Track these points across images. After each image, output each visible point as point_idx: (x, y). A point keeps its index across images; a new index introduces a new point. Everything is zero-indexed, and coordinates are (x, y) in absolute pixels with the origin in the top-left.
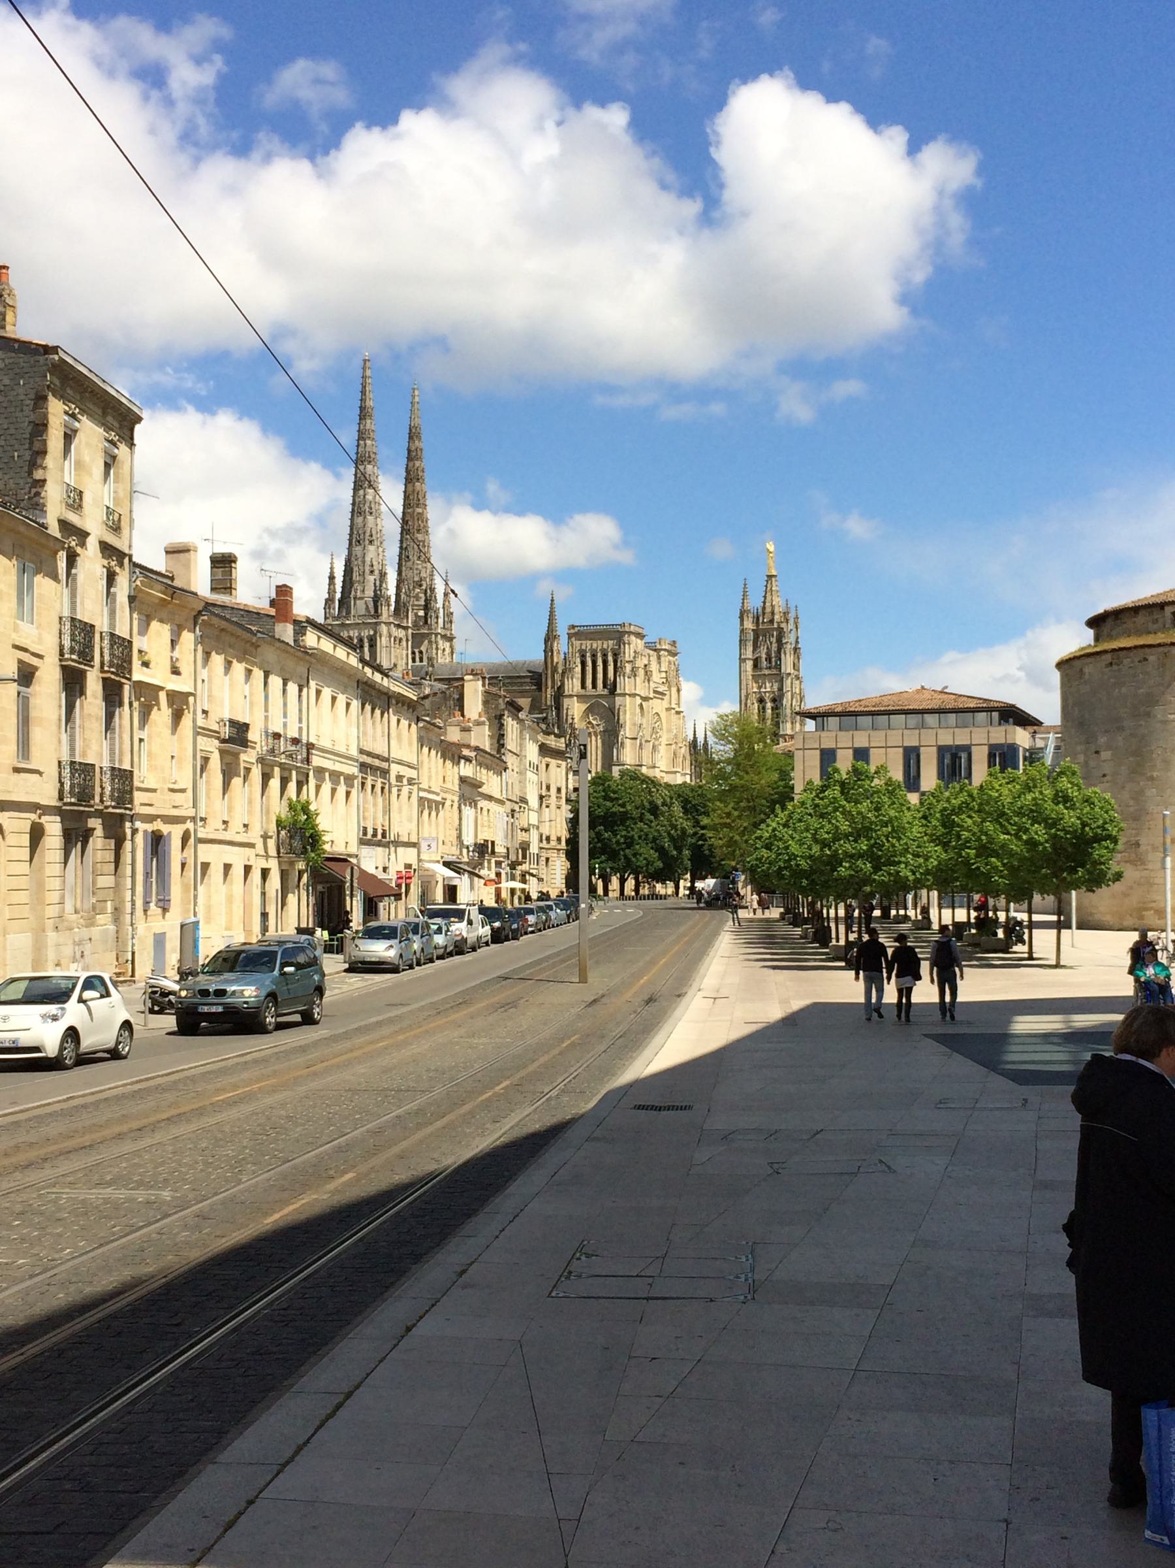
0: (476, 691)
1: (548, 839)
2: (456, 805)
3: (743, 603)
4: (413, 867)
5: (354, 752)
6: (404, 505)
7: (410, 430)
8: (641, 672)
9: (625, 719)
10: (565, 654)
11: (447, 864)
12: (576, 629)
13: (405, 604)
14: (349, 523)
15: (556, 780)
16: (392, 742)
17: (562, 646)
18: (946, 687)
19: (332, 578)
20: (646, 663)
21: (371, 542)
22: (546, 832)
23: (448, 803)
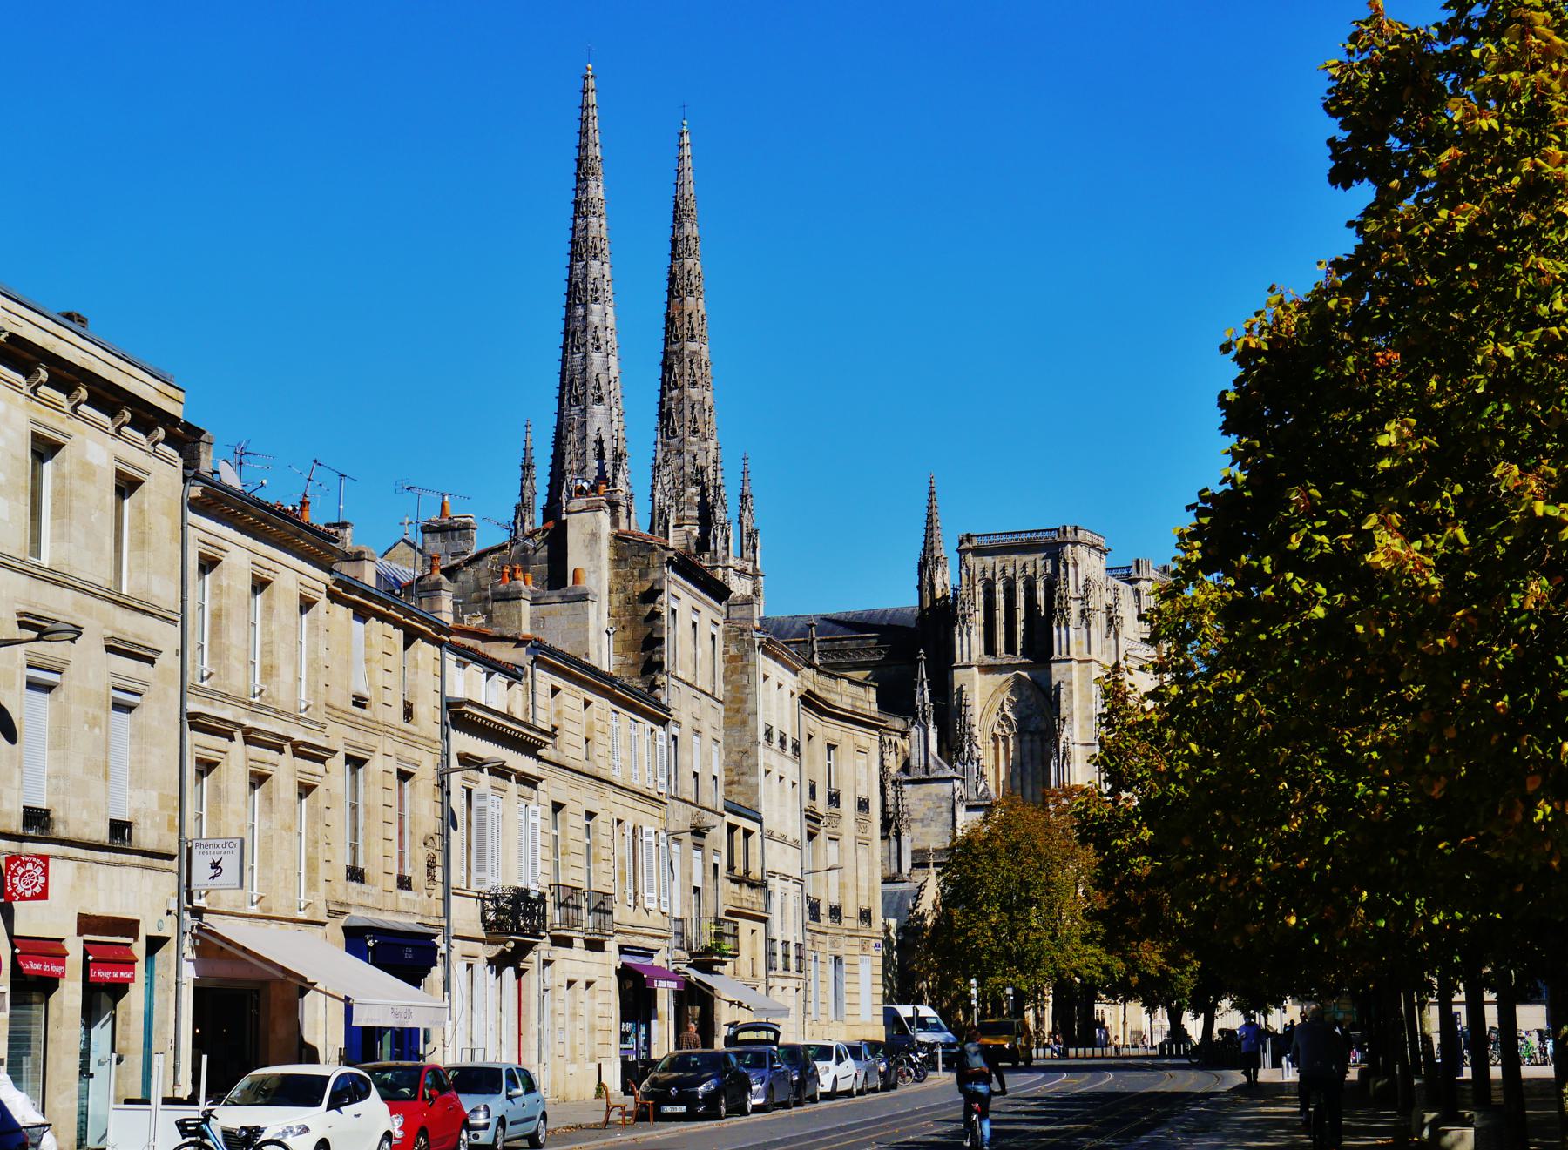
0: (594, 536)
1: (836, 912)
6: (666, 340)
7: (677, 206)
8: (1099, 619)
9: (1070, 707)
10: (954, 589)
11: (357, 940)
12: (975, 541)
13: (662, 512)
17: (945, 580)
19: (527, 467)
20: (1111, 602)
21: (600, 400)
22: (828, 896)
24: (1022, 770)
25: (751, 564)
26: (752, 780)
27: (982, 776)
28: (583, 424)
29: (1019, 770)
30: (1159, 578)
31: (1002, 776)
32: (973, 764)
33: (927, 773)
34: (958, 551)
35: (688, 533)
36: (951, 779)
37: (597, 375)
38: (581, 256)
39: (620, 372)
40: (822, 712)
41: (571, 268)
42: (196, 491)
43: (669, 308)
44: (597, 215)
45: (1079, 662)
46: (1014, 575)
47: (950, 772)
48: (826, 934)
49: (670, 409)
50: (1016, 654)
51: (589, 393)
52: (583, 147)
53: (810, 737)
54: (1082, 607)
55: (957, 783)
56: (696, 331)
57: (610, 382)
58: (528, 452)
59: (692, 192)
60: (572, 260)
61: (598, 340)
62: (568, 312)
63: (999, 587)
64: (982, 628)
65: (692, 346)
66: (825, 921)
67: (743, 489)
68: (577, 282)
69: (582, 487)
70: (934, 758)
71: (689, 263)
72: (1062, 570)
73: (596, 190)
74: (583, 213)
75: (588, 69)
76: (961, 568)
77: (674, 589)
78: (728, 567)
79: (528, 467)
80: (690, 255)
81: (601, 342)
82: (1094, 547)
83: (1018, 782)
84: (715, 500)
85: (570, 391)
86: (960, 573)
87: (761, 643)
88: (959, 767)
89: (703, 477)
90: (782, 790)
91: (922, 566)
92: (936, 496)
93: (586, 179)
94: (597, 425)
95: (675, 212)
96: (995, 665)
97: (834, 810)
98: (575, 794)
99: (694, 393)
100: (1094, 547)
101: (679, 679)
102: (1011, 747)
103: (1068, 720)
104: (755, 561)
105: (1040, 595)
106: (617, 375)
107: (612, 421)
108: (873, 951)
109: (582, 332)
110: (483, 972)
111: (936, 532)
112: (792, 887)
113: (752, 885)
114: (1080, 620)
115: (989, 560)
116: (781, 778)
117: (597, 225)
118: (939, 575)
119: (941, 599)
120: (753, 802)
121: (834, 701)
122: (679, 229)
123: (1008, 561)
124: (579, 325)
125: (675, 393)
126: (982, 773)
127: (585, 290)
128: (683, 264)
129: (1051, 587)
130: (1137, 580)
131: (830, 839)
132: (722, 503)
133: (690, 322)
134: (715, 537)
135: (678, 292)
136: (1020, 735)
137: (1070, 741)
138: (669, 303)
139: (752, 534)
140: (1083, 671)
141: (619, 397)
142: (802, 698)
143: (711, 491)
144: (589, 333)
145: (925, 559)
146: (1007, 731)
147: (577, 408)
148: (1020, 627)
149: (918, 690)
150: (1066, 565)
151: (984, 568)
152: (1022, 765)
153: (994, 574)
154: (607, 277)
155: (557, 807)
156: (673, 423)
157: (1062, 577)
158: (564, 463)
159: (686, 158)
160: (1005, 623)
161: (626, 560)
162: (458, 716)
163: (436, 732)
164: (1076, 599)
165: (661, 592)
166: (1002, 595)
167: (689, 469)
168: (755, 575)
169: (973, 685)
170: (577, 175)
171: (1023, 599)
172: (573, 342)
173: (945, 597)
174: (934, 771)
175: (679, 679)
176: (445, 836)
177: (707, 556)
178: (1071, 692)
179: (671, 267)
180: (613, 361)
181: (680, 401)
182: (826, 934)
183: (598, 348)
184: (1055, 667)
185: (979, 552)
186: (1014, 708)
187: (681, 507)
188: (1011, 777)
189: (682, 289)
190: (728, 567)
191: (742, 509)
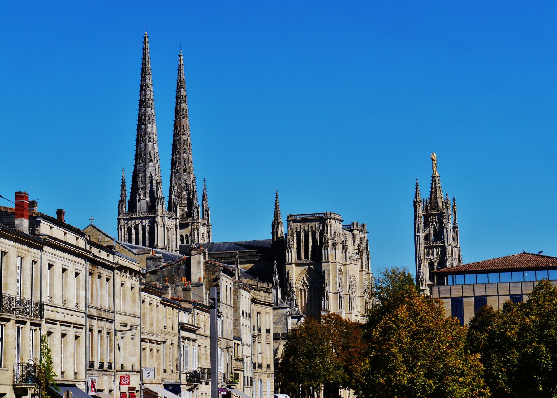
0: (199, 262)
1: (260, 366)
2: (176, 343)
3: (416, 197)
4: (136, 389)
5: (82, 307)
6: (174, 135)
7: (178, 83)
8: (339, 246)
9: (329, 279)
10: (286, 235)
11: (166, 387)
12: (294, 217)
13: (175, 203)
14: (135, 148)
15: (266, 324)
16: (117, 301)
17: (283, 230)
18: (541, 252)
19: (123, 186)
20: (344, 239)
21: (151, 161)
22: (258, 361)
23: (168, 342)
24: (311, 303)
25: (207, 221)
26: (239, 328)
27: (297, 306)
28: (145, 170)
29: (310, 302)
30: (361, 229)
31: (303, 305)
32: (293, 301)
33: (277, 305)
34: (287, 220)
36: (286, 308)
37: (150, 152)
38: (144, 106)
39: (158, 150)
40: (256, 303)
41: (140, 110)
42: (143, 287)
43: (175, 123)
44: (150, 90)
45: (332, 262)
46: (308, 230)
47: (286, 305)
48: (257, 373)
49: (176, 162)
51: (147, 159)
52: (144, 64)
53: (253, 311)
54: (333, 242)
55: (288, 309)
56: (186, 132)
57: (155, 154)
58: (123, 180)
59: (184, 78)
60: (140, 107)
61: (150, 138)
62: (138, 127)
63: (302, 234)
64: (296, 250)
65: (185, 138)
66: (257, 369)
67: (204, 192)
68: (142, 116)
69: (195, 247)
70: (280, 300)
71: (183, 106)
72: (326, 229)
74: (144, 89)
75: (145, 34)
76: (288, 227)
77: (222, 277)
78: (198, 223)
79: (123, 186)
80: (183, 103)
81: (151, 139)
82: (338, 219)
83: (309, 307)
84: (193, 197)
85: (140, 158)
86: (288, 229)
87: (241, 286)
88: (289, 302)
89: (188, 188)
90: (246, 329)
91: (273, 225)
92: (279, 199)
93: (145, 77)
94: (150, 171)
95: (177, 86)
96: (301, 263)
97: (259, 333)
98: (202, 342)
99: (185, 156)
100: (338, 219)
101: (223, 303)
102: (307, 294)
103: (328, 284)
104: (208, 220)
105: (318, 237)
106: (157, 151)
107: (156, 169)
108: (271, 378)
109: (144, 135)
110: (186, 392)
111: (278, 213)
112: (249, 359)
113: (240, 361)
114: (332, 247)
115: (299, 224)
116: (246, 326)
117: (149, 94)
118: (280, 228)
119: (280, 237)
120: (239, 335)
121: (259, 299)
122: (179, 92)
123: (306, 225)
124: (143, 133)
125: (178, 156)
126: (297, 305)
127: (145, 119)
128: (181, 106)
129: (322, 234)
130: (353, 230)
131: (258, 343)
132: (196, 198)
133: (183, 129)
135: (179, 117)
137: (329, 292)
138: (175, 121)
139: (207, 210)
140: (334, 266)
141: (158, 160)
142: (251, 300)
143: (192, 194)
144: (147, 135)
146: (305, 288)
147: (142, 164)
148: (310, 249)
149: (274, 275)
151: (297, 227)
152: (311, 300)
153: (300, 230)
154: (154, 114)
155: (199, 346)
156: (177, 167)
157: (326, 231)
158: (137, 185)
159: (181, 65)
160: (305, 248)
161: (208, 269)
162: (182, 327)
163: (176, 331)
164: (331, 239)
165: (219, 279)
166: (303, 237)
167: (183, 185)
168: (208, 225)
169: (293, 270)
170: (142, 75)
171: (311, 239)
172: (141, 139)
173: (282, 237)
174: (280, 305)
175: (223, 303)
176: (179, 358)
177: (191, 218)
178: (329, 274)
179: (176, 107)
180: (156, 146)
181: (180, 159)
182: (257, 373)
183: (150, 141)
184: (323, 264)
185: (295, 221)
186: (307, 280)
187: (180, 199)
188: (307, 304)
189: (180, 116)
190: (198, 223)
191: (203, 200)
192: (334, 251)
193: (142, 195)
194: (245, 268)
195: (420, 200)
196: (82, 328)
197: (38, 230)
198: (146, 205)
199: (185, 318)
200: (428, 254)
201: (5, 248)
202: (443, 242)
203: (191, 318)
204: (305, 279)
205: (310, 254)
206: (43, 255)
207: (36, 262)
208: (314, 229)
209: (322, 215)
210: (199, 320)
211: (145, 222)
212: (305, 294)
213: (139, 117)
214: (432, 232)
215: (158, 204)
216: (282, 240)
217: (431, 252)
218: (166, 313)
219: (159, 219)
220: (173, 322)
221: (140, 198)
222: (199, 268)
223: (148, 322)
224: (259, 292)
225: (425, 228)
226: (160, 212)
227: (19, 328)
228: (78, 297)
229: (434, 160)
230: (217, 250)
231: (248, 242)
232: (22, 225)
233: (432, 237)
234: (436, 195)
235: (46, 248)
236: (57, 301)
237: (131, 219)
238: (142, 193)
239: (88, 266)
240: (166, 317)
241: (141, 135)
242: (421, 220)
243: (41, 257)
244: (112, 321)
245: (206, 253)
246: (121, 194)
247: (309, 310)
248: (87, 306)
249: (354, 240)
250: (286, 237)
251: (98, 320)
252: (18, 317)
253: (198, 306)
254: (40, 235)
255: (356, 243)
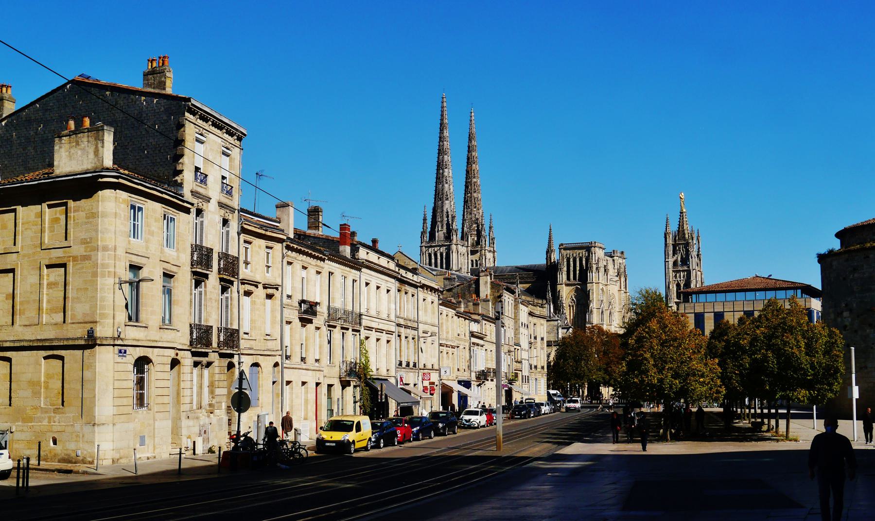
0: (486, 282)
1: (536, 367)
2: (467, 348)
3: (666, 229)
4: (436, 384)
5: (393, 318)
6: (466, 178)
7: (470, 135)
8: (602, 270)
9: (593, 297)
11: (460, 382)
12: (564, 246)
13: (466, 234)
14: (434, 188)
15: (541, 333)
17: (555, 257)
18: (771, 276)
19: (425, 220)
21: (447, 199)
22: (534, 363)
23: (461, 347)
27: (566, 318)
28: (443, 207)
31: (572, 318)
33: (550, 318)
35: (473, 239)
36: (557, 320)
40: (533, 316)
41: (438, 158)
42: (441, 302)
43: (467, 168)
47: (557, 318)
50: (576, 280)
51: (444, 197)
52: (442, 120)
55: (559, 321)
60: (438, 155)
63: (571, 260)
65: (475, 180)
66: (533, 369)
71: (473, 154)
72: (591, 255)
73: (446, 133)
77: (505, 295)
82: (601, 248)
83: (576, 320)
84: (482, 229)
85: (438, 196)
91: (547, 252)
93: (443, 130)
95: (469, 137)
98: (489, 347)
100: (601, 248)
105: (584, 262)
108: (544, 377)
110: (476, 387)
112: (527, 362)
113: (519, 363)
115: (568, 251)
124: (441, 176)
125: (469, 195)
127: (443, 165)
134: (482, 240)
136: (577, 306)
138: (467, 166)
142: (529, 313)
143: (481, 226)
145: (548, 249)
148: (578, 272)
149: (548, 293)
150: (592, 254)
151: (567, 254)
152: (578, 314)
153: (570, 256)
155: (486, 350)
157: (591, 257)
162: (472, 335)
168: (494, 252)
170: (440, 128)
173: (554, 262)
176: (470, 360)
177: (479, 246)
179: (468, 155)
180: (451, 186)
181: (471, 197)
183: (447, 183)
184: (588, 285)
185: (565, 249)
191: (490, 231)
192: (597, 274)
193: (440, 227)
194: (523, 287)
195: (670, 231)
196: (392, 334)
197: (357, 255)
198: (443, 235)
199: (475, 327)
200: (676, 276)
201: (333, 269)
202: (689, 267)
203: (479, 327)
204: (573, 297)
205: (577, 276)
206: (361, 276)
207: (356, 281)
208: (581, 255)
209: (588, 244)
210: (486, 329)
211: (443, 249)
212: (573, 309)
213: (438, 163)
214: (679, 259)
215: (453, 234)
216: (555, 264)
217: (678, 275)
218: (459, 323)
219: (454, 247)
220: (465, 330)
221: (438, 230)
222: (486, 287)
223: (445, 330)
224: (535, 307)
225: (674, 255)
226: (454, 241)
227: (343, 333)
228: (389, 309)
229: (682, 199)
230: (501, 273)
231: (526, 266)
232: (345, 251)
233: (680, 263)
234: (683, 228)
235: (364, 270)
236: (373, 313)
237: (431, 247)
238: (440, 225)
239: (397, 284)
240: (459, 326)
241: (440, 178)
242: (671, 248)
243: (360, 277)
244: (416, 329)
245: (492, 274)
246: (423, 226)
247: (577, 323)
248: (397, 317)
249: (614, 265)
250: (558, 262)
251: (405, 328)
252: (343, 325)
253: (486, 318)
254: (359, 259)
255: (616, 267)
